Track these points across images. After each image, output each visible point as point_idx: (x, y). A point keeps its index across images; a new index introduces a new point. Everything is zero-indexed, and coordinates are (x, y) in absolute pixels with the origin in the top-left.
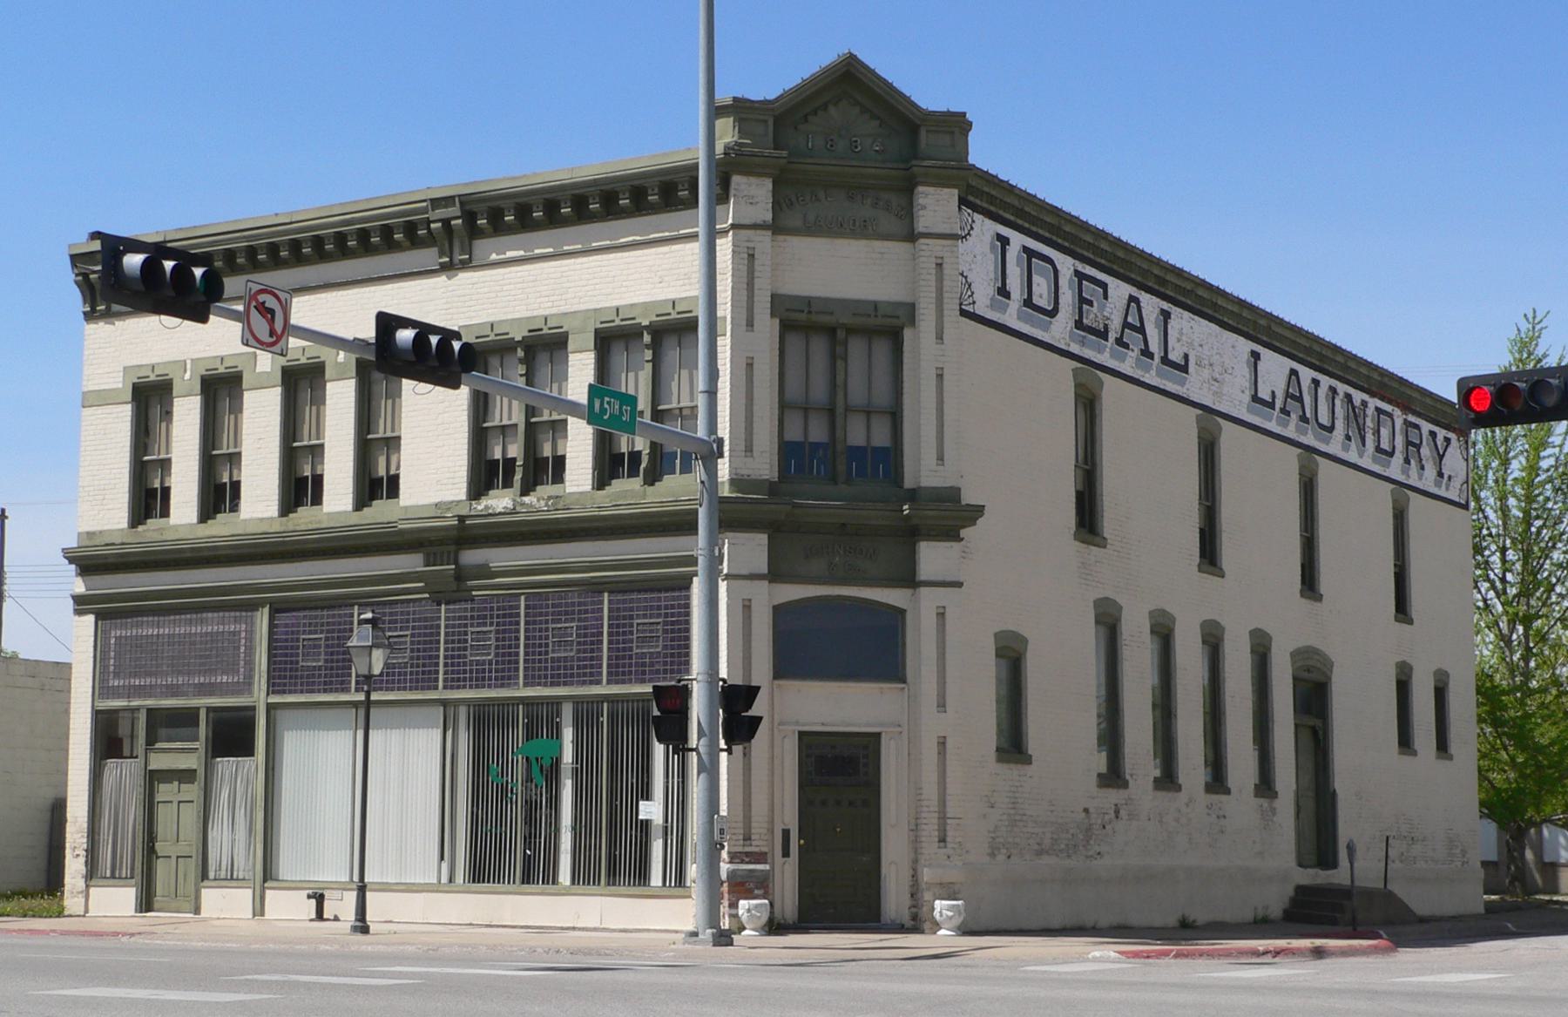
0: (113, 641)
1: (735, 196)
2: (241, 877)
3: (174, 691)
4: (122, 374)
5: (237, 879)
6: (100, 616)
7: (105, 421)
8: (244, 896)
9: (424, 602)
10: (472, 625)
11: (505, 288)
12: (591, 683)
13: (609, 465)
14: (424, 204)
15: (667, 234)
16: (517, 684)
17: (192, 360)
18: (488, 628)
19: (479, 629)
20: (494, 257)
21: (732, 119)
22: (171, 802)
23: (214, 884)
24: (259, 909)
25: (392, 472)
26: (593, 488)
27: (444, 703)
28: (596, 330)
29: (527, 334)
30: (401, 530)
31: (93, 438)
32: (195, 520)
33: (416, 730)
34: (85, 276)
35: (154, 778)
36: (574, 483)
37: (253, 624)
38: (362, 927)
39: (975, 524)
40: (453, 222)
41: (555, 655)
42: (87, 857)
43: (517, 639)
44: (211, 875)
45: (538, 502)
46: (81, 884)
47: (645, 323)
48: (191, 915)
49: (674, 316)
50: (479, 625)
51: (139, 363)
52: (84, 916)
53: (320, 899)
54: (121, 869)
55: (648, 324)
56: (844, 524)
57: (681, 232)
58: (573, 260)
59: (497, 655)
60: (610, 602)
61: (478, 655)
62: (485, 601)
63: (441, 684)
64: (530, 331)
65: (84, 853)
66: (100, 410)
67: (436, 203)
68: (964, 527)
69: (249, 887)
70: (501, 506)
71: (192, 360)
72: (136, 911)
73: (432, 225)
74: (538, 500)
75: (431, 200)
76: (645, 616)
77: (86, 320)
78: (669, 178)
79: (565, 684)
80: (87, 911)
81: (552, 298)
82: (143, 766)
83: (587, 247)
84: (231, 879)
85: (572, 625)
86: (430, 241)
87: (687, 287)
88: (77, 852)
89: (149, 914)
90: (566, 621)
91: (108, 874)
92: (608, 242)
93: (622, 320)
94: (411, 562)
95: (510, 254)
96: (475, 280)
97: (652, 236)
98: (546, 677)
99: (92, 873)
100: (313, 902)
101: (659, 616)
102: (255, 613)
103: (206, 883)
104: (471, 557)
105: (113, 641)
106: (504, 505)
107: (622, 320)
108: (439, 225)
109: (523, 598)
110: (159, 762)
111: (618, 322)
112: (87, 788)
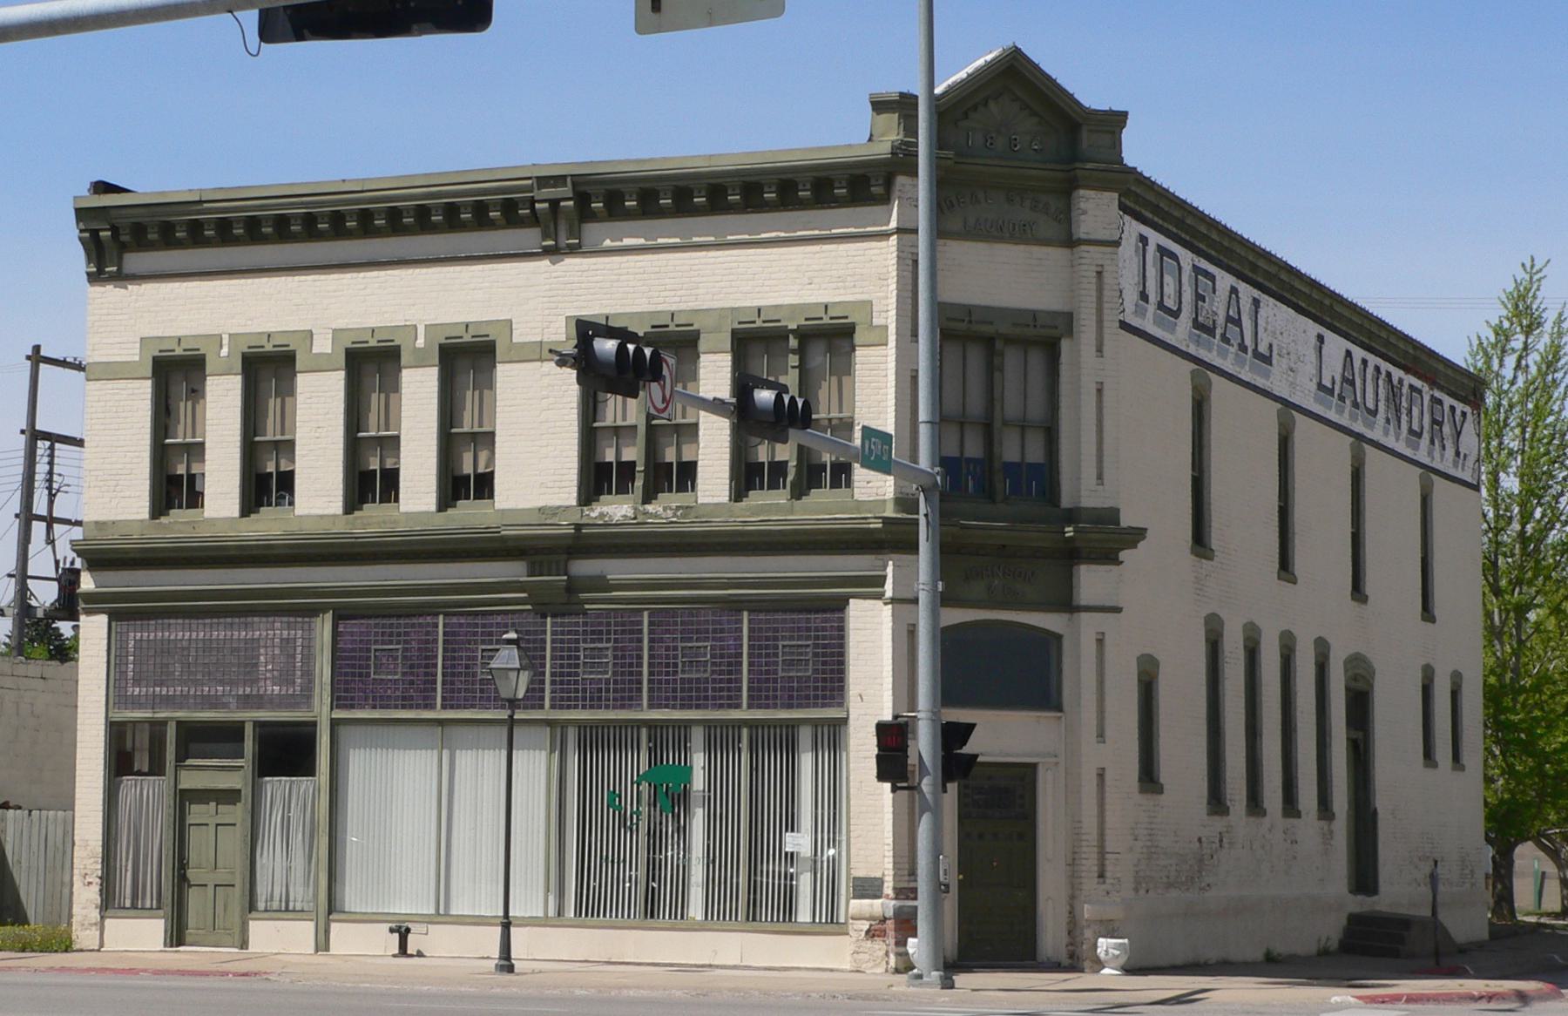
0: (131, 644)
1: (899, 198)
2: (298, 907)
3: (213, 703)
4: (138, 345)
5: (294, 911)
6: (114, 616)
7: (117, 397)
8: (303, 932)
9: (525, 614)
10: (585, 641)
11: (622, 278)
12: (730, 706)
13: (746, 476)
14: (530, 182)
15: (817, 232)
16: (640, 705)
17: (230, 335)
19: (592, 645)
20: (608, 243)
21: (897, 115)
22: (207, 825)
23: (266, 915)
24: (322, 944)
25: (481, 470)
26: (730, 500)
27: (550, 723)
29: (650, 330)
30: (502, 537)
31: (102, 415)
32: (236, 514)
34: (95, 233)
35: (185, 798)
36: (707, 493)
38: (506, 963)
39: (1135, 547)
40: (562, 204)
41: (686, 676)
42: (101, 885)
43: (640, 657)
44: (261, 905)
45: (664, 510)
46: (95, 915)
47: (792, 326)
48: (236, 950)
49: (826, 320)
50: (593, 641)
51: (160, 335)
52: (99, 950)
53: (403, 934)
54: (144, 898)
55: (795, 327)
56: (1004, 546)
57: (834, 231)
58: (704, 253)
59: (615, 673)
60: (750, 621)
61: (591, 673)
62: (599, 616)
63: (547, 703)
64: (653, 327)
65: (99, 881)
66: (110, 384)
67: (543, 181)
68: (1123, 549)
69: (312, 920)
70: (619, 515)
71: (230, 335)
72: (165, 945)
73: (537, 205)
74: (665, 509)
75: (538, 178)
76: (792, 638)
77: (89, 282)
79: (698, 707)
80: (102, 945)
81: (679, 293)
82: (172, 783)
83: (720, 240)
84: (286, 910)
85: (706, 644)
86: (534, 220)
87: (842, 291)
89: (181, 948)
90: (698, 640)
91: (128, 904)
92: (747, 237)
93: (764, 322)
95: (628, 242)
96: (586, 267)
98: (675, 698)
99: (109, 902)
100: (396, 935)
101: (808, 638)
102: (313, 620)
103: (254, 914)
104: (585, 567)
105: (131, 644)
106: (623, 513)
107: (764, 322)
108: (546, 205)
109: (646, 614)
110: (189, 781)
111: (759, 324)
112: (101, 808)
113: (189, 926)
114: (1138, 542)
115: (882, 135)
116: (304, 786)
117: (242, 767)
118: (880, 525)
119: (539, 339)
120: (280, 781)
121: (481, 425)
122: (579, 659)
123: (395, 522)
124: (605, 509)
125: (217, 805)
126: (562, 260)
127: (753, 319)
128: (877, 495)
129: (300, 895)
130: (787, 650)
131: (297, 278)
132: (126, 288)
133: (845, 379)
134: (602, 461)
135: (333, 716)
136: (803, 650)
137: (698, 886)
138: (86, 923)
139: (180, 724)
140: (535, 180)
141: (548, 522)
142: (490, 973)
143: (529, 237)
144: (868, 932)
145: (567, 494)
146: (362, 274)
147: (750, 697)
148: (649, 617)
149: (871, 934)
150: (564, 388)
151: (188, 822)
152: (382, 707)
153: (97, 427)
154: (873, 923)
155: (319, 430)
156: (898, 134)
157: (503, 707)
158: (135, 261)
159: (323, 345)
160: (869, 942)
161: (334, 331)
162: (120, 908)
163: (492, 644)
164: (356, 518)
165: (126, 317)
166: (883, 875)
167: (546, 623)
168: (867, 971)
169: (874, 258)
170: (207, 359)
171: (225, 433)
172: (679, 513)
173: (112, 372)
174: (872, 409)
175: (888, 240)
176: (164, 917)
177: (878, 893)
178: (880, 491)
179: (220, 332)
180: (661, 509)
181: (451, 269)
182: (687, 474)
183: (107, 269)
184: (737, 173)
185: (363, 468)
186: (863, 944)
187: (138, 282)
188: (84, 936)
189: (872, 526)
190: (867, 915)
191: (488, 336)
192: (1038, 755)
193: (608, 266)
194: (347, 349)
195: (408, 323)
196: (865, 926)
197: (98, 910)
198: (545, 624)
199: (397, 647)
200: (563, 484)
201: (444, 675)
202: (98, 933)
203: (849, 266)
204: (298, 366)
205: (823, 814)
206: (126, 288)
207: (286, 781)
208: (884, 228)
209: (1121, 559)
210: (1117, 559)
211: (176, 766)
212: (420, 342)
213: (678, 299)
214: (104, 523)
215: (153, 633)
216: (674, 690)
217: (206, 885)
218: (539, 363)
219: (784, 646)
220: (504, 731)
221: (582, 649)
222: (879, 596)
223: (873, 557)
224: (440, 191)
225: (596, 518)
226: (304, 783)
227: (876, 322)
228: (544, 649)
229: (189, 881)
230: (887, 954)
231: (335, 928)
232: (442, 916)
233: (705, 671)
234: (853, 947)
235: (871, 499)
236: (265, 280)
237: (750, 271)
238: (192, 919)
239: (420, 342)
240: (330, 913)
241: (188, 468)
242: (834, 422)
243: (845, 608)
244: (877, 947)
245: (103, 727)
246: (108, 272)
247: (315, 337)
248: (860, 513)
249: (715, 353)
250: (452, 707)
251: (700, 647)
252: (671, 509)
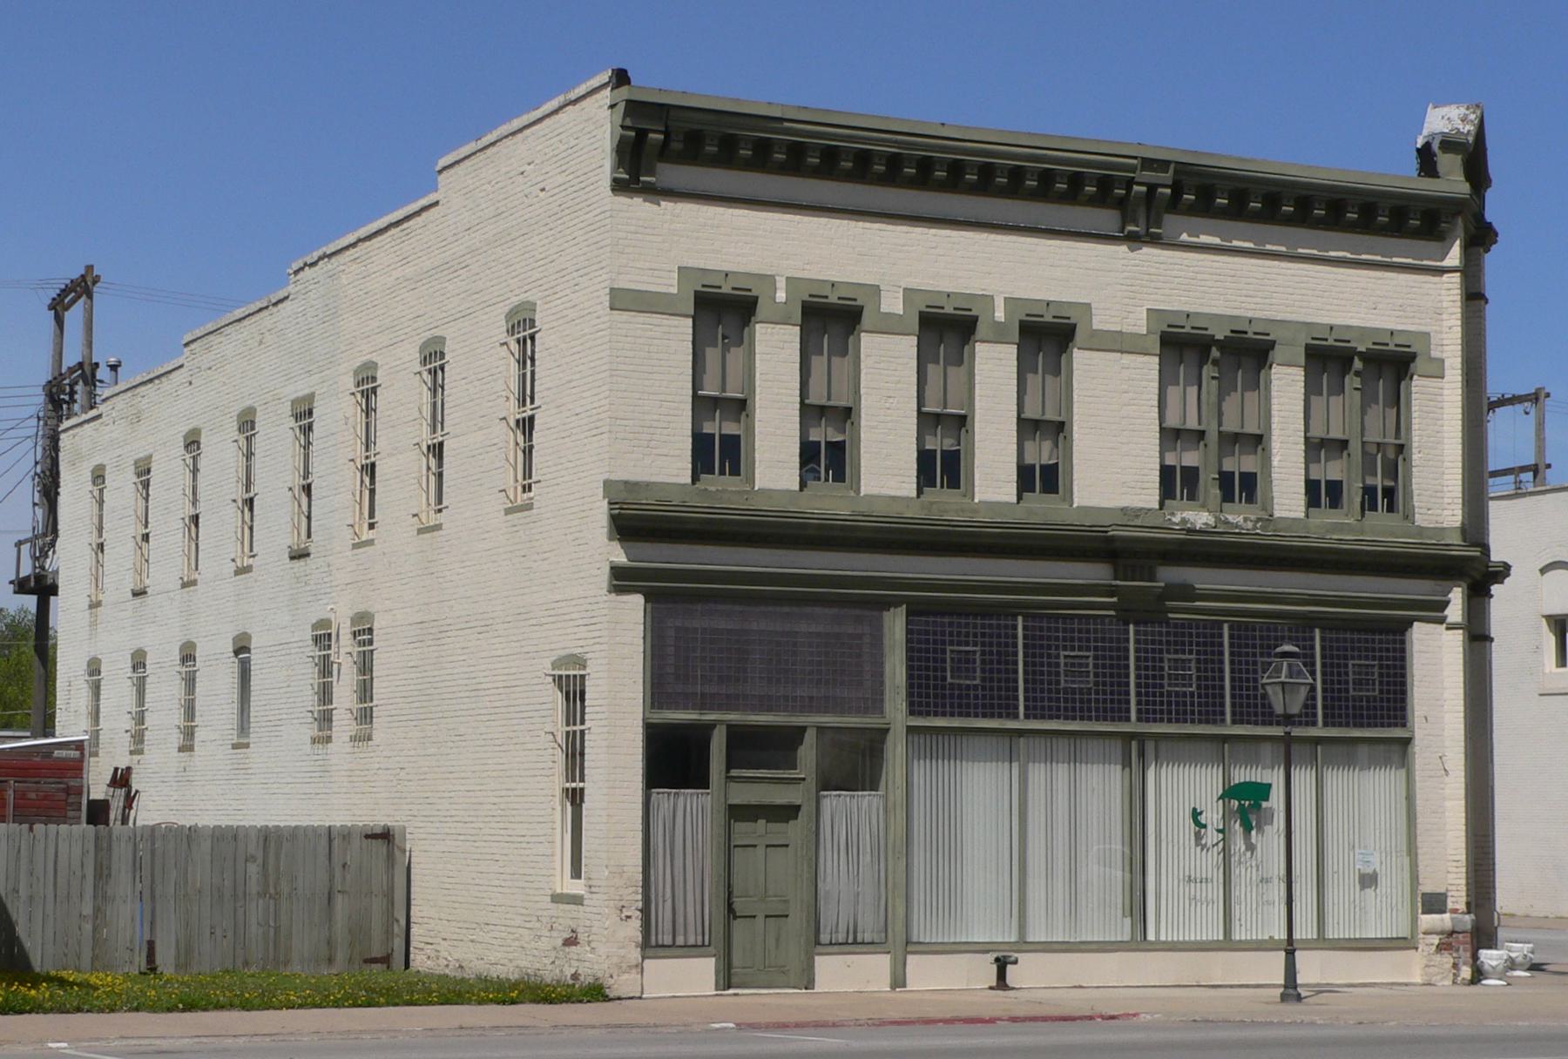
2: (868, 938)
3: (765, 705)
5: (863, 943)
6: (650, 596)
7: (649, 334)
9: (1107, 620)
10: (1168, 652)
12: (1307, 724)
14: (1135, 162)
16: (1223, 721)
18: (1187, 656)
19: (1176, 656)
20: (1184, 237)
22: (755, 846)
23: (830, 949)
24: (898, 981)
27: (1128, 737)
28: (1306, 345)
29: (1229, 334)
30: (1113, 536)
33: (982, 764)
34: (642, 134)
35: (737, 813)
36: (1285, 507)
37: (880, 628)
38: (1291, 989)
40: (1160, 190)
43: (1222, 671)
44: (824, 938)
45: (1239, 517)
46: (635, 954)
47: (1362, 348)
48: (804, 991)
50: (1176, 652)
51: (702, 266)
52: (640, 998)
53: (1002, 965)
58: (1276, 263)
59: (1199, 687)
60: (1323, 639)
62: (1183, 626)
64: (1232, 331)
66: (642, 318)
67: (1148, 163)
69: (889, 952)
73: (1136, 188)
74: (1246, 520)
75: (1142, 158)
76: (1360, 658)
82: (723, 800)
84: (853, 943)
86: (1121, 204)
88: (626, 913)
89: (731, 991)
92: (1315, 252)
94: (1094, 573)
95: (1205, 239)
96: (1162, 259)
101: (1374, 658)
103: (819, 949)
104: (1170, 574)
106: (1205, 521)
107: (1336, 340)
108: (1144, 189)
109: (1226, 627)
110: (744, 795)
111: (1330, 342)
117: (804, 779)
118: (1478, 554)
119: (1119, 329)
120: (839, 796)
132: (659, 205)
142: (1276, 1003)
143: (1107, 218)
144: (1437, 947)
145: (1149, 497)
146: (933, 231)
147: (1325, 716)
148: (1024, 621)
149: (1440, 948)
153: (623, 367)
155: (891, 400)
157: (1278, 724)
158: (670, 174)
159: (892, 304)
162: (658, 946)
166: (1447, 890)
171: (781, 391)
172: (1258, 525)
176: (715, 956)
182: (1246, 487)
183: (642, 179)
186: (1433, 957)
190: (1439, 929)
191: (1069, 318)
196: (1435, 940)
197: (639, 949)
198: (1127, 632)
200: (1146, 485)
201: (1026, 681)
206: (659, 205)
208: (1438, 264)
214: (636, 484)
216: (1256, 706)
217: (754, 917)
218: (1119, 354)
219: (1353, 665)
222: (1441, 621)
224: (1045, 155)
228: (1127, 658)
230: (1455, 966)
231: (912, 960)
232: (1024, 945)
234: (1425, 961)
235: (1432, 526)
236: (823, 220)
243: (1406, 630)
244: (1445, 960)
245: (640, 730)
246: (644, 182)
250: (1035, 717)
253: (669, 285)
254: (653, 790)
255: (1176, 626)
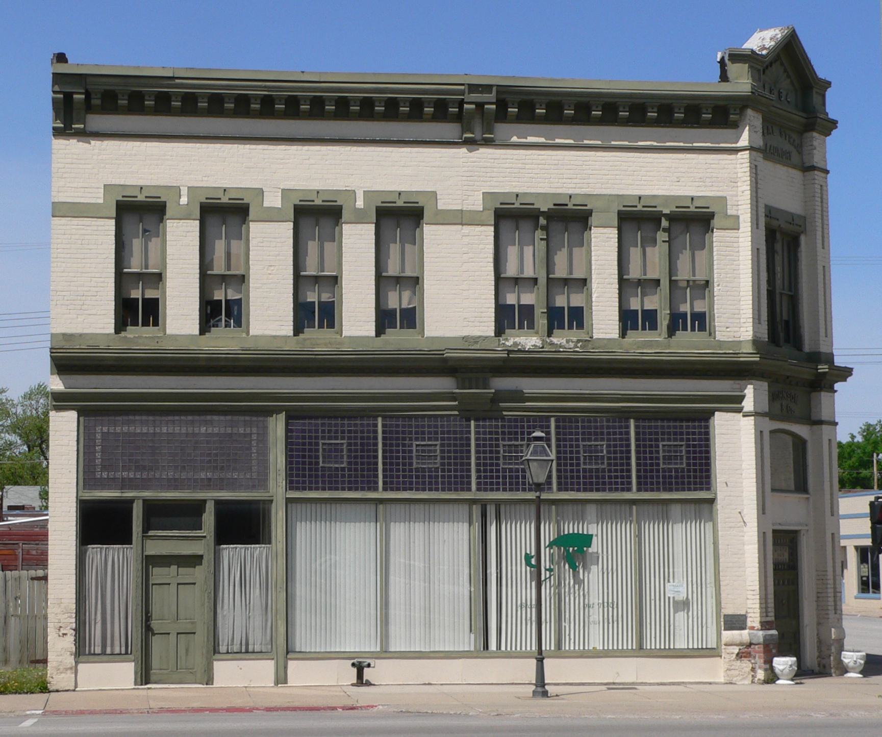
0: (99, 436)
1: (749, 124)
2: (257, 649)
3: (175, 484)
4: (102, 191)
5: (253, 652)
6: (81, 412)
8: (264, 670)
10: (503, 439)
11: (527, 166)
12: (623, 490)
13: (628, 320)
14: (462, 87)
15: (682, 144)
17: (188, 187)
18: (519, 442)
20: (515, 139)
21: (747, 65)
24: (281, 678)
25: (404, 305)
26: (619, 337)
27: (473, 502)
28: (618, 211)
30: (446, 357)
31: (68, 246)
32: (197, 332)
34: (68, 97)
35: (150, 562)
36: (601, 331)
37: (265, 428)
38: (541, 687)
39: (845, 380)
41: (588, 467)
42: (75, 636)
44: (223, 649)
46: (71, 660)
48: (205, 686)
49: (692, 209)
50: (510, 439)
52: (74, 690)
53: (360, 669)
54: (112, 645)
55: (669, 212)
56: (788, 377)
57: (695, 145)
58: (593, 153)
60: (637, 427)
62: (516, 421)
63: (474, 486)
64: (555, 205)
65: (74, 633)
67: (473, 88)
68: (837, 382)
69: (273, 659)
70: (530, 344)
71: (188, 187)
72: (136, 684)
73: (466, 106)
74: (568, 341)
75: (468, 84)
76: (669, 440)
77: (54, 135)
78: (697, 102)
79: (598, 490)
80: (76, 686)
81: (575, 181)
82: (140, 552)
83: (606, 144)
84: (246, 652)
85: (602, 443)
86: (458, 117)
87: (703, 189)
88: (63, 631)
89: (149, 686)
90: (596, 440)
91: (98, 650)
92: (627, 143)
93: (644, 207)
94: (443, 384)
95: (531, 139)
97: (668, 144)
99: (82, 651)
100: (355, 670)
101: (682, 440)
102: (266, 419)
103: (217, 656)
105: (99, 436)
107: (644, 207)
108: (473, 106)
109: (553, 420)
110: (155, 548)
111: (640, 208)
112: (74, 572)
113: (153, 667)
114: (847, 377)
115: (737, 79)
116: (258, 552)
117: (205, 537)
118: (758, 359)
119: (460, 208)
120: (236, 548)
121: (229, 268)
122: (499, 453)
123: (340, 344)
124: (517, 339)
125: (178, 567)
126: (478, 150)
127: (634, 204)
128: (734, 337)
129: (257, 641)
130: (666, 448)
131: (248, 146)
132: (90, 143)
133: (328, 246)
134: (554, 306)
135: (287, 496)
136: (432, 448)
137: (595, 624)
138: (61, 668)
139: (146, 503)
140: (467, 86)
141: (470, 348)
142: (529, 698)
143: (450, 130)
144: (737, 655)
145: (488, 328)
146: (306, 148)
147: (639, 483)
149: (739, 656)
150: (481, 246)
151: (151, 583)
152: (330, 489)
153: (62, 255)
154: (741, 647)
155: (272, 268)
156: (748, 79)
157: (530, 490)
158: (97, 121)
159: (273, 200)
160: (739, 661)
161: (283, 190)
162: (90, 654)
163: (338, 439)
164: (305, 340)
165: (89, 166)
166: (747, 612)
167: (470, 425)
168: (737, 683)
169: (726, 166)
170: (168, 205)
171: (184, 266)
172: (579, 345)
173: (460, 218)
174: (728, 275)
175: (737, 154)
176: (134, 661)
177: (744, 626)
178: (735, 334)
179: (178, 185)
180: (565, 342)
181: (384, 149)
182: (578, 317)
183: (73, 126)
184: (630, 96)
185: (125, 296)
186: (734, 663)
187: (102, 139)
188: (57, 676)
189: (742, 359)
190: (738, 642)
191: (417, 203)
192: (801, 524)
193: (516, 157)
194: (117, 201)
195: (347, 188)
196: (736, 650)
197: (73, 657)
198: (469, 426)
199: (342, 441)
200: (485, 319)
201: (384, 464)
202: (73, 675)
203: (708, 170)
204: (251, 217)
205: (512, 570)
206: (90, 143)
207: (241, 548)
208: (734, 145)
209: (835, 389)
210: (833, 388)
211: (143, 536)
212: (184, 200)
213: (574, 186)
214: (72, 335)
215: (122, 428)
216: (578, 477)
217: (169, 634)
218: (461, 226)
219: (664, 446)
220: (533, 508)
221: (501, 446)
222: (739, 410)
223: (731, 382)
224: (387, 88)
225: (510, 347)
226: (257, 550)
227: (730, 212)
228: (469, 445)
229: (152, 630)
230: (753, 669)
231: (292, 664)
232: (385, 653)
233: (602, 463)
234: (726, 666)
235: (730, 340)
236: (218, 146)
237: (630, 169)
238: (155, 662)
239: (184, 200)
240: (287, 653)
241: (143, 294)
242: (691, 283)
243: (710, 418)
244: (745, 665)
245: (75, 505)
246: (74, 128)
247: (265, 193)
248: (722, 350)
249: (483, 225)
250: (392, 489)
251: (597, 445)
252: (573, 342)
253: (98, 197)
254: (89, 546)
255: (510, 421)
